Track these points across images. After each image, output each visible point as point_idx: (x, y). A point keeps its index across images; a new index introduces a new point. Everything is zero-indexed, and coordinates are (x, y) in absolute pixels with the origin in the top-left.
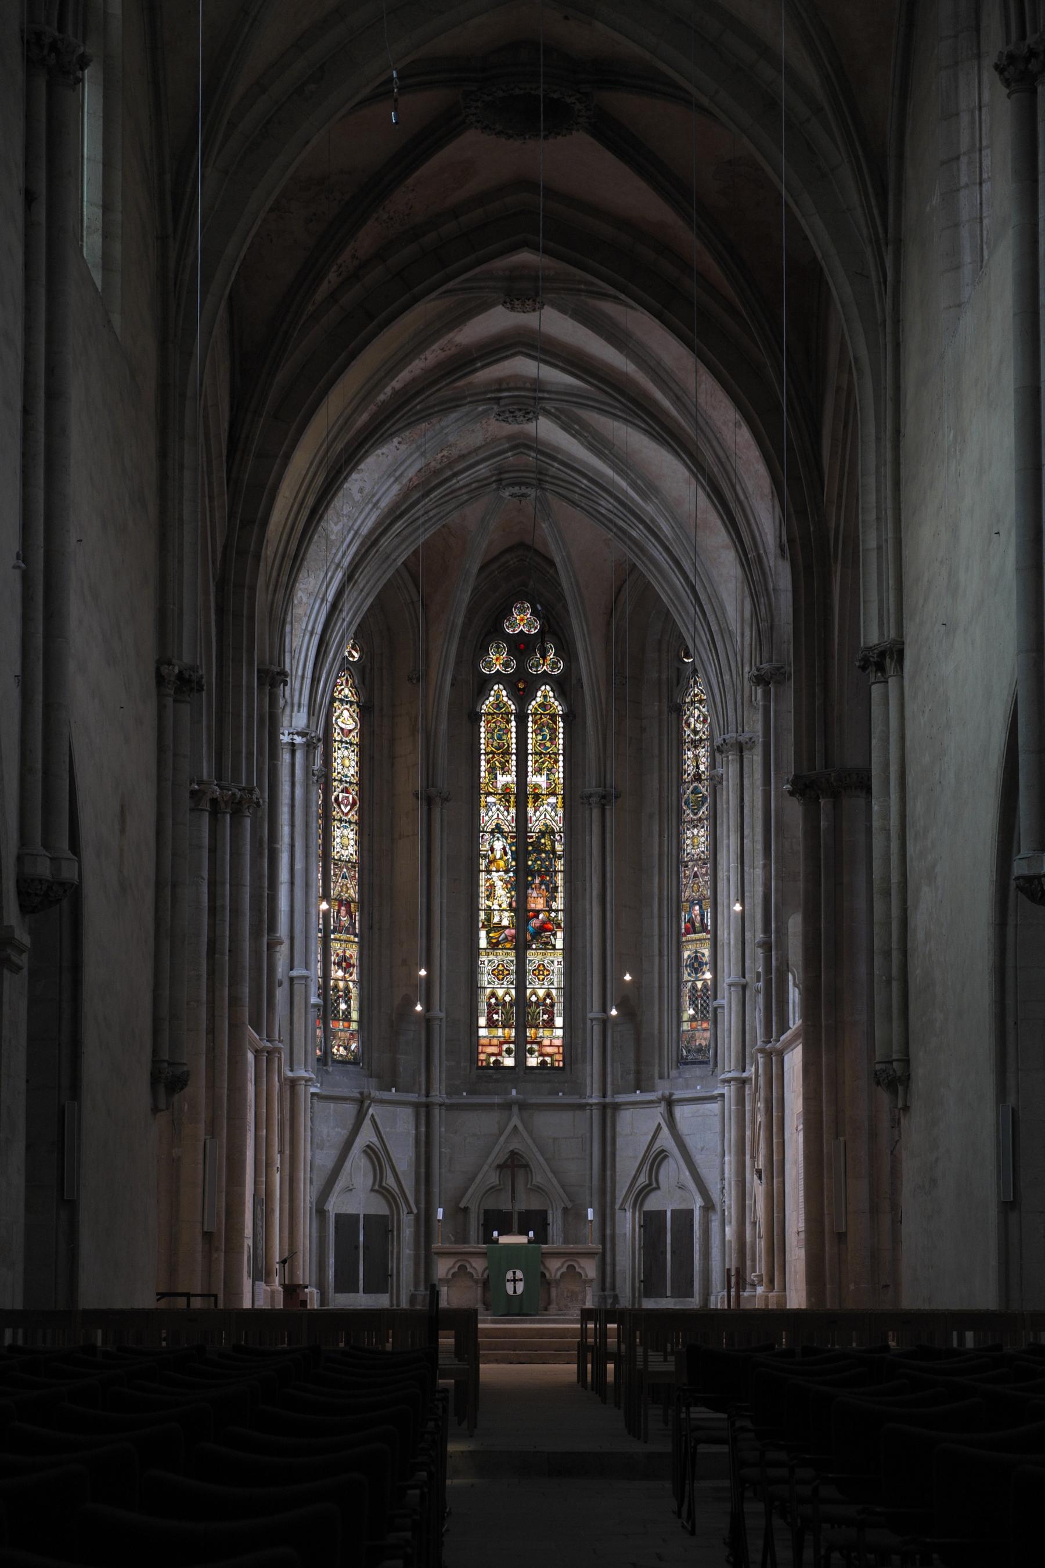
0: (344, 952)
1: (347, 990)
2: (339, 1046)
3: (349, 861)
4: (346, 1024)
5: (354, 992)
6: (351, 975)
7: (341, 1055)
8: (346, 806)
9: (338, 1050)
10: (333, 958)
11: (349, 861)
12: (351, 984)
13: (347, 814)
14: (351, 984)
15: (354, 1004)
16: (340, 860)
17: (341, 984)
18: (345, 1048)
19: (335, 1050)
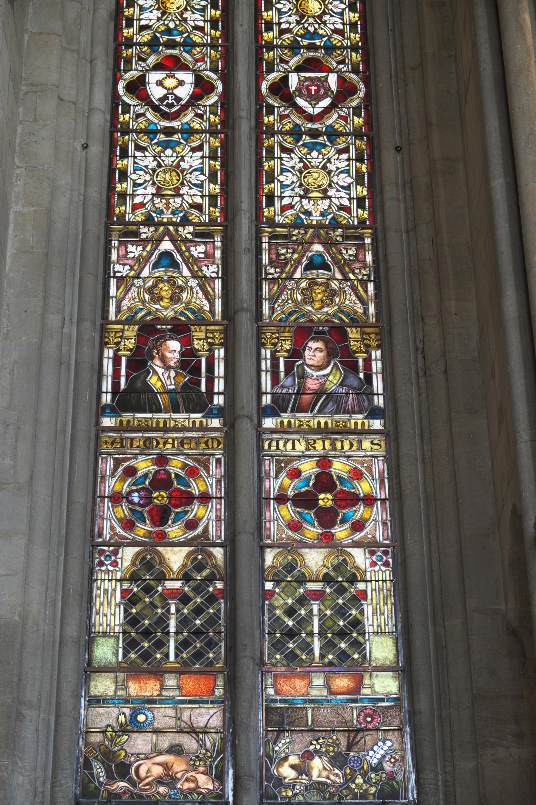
0: (324, 462)
1: (342, 579)
2: (308, 756)
3: (335, 224)
4: (342, 683)
5: (376, 576)
6: (358, 526)
7: (320, 787)
8: (314, 99)
9: (302, 769)
10: (272, 486)
11: (335, 224)
12: (359, 557)
13: (319, 117)
14: (359, 557)
15: (378, 615)
16: (297, 224)
17: (315, 560)
18: (338, 760)
19: (287, 772)
